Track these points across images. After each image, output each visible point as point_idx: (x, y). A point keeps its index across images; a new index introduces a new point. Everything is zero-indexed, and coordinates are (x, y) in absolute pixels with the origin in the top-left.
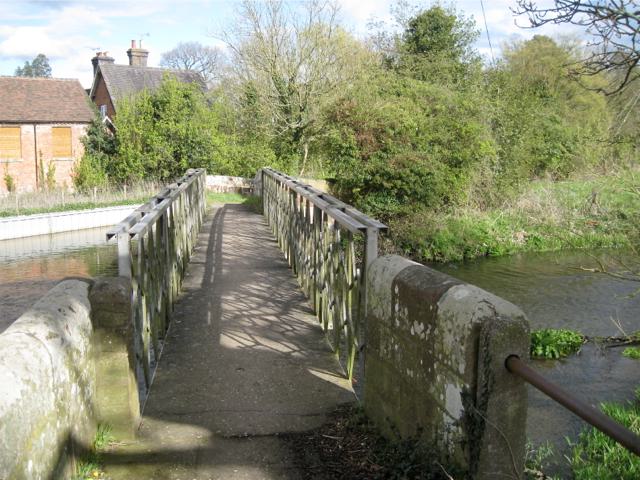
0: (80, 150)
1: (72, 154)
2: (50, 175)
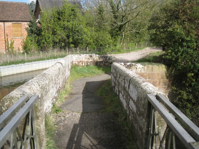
0: (26, 33)
1: (22, 35)
2: (12, 44)
